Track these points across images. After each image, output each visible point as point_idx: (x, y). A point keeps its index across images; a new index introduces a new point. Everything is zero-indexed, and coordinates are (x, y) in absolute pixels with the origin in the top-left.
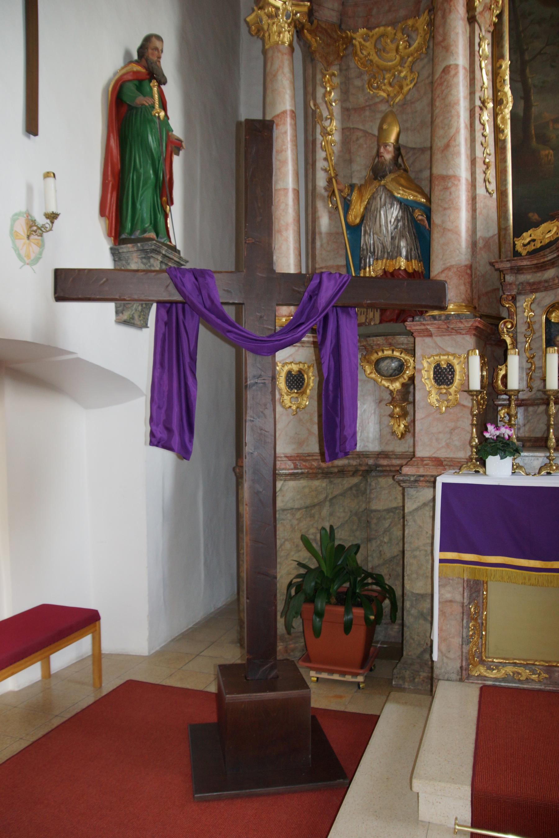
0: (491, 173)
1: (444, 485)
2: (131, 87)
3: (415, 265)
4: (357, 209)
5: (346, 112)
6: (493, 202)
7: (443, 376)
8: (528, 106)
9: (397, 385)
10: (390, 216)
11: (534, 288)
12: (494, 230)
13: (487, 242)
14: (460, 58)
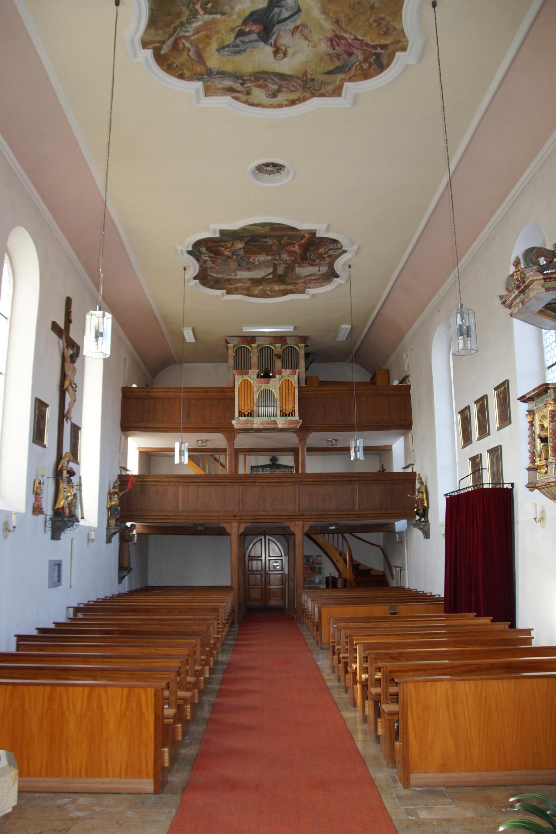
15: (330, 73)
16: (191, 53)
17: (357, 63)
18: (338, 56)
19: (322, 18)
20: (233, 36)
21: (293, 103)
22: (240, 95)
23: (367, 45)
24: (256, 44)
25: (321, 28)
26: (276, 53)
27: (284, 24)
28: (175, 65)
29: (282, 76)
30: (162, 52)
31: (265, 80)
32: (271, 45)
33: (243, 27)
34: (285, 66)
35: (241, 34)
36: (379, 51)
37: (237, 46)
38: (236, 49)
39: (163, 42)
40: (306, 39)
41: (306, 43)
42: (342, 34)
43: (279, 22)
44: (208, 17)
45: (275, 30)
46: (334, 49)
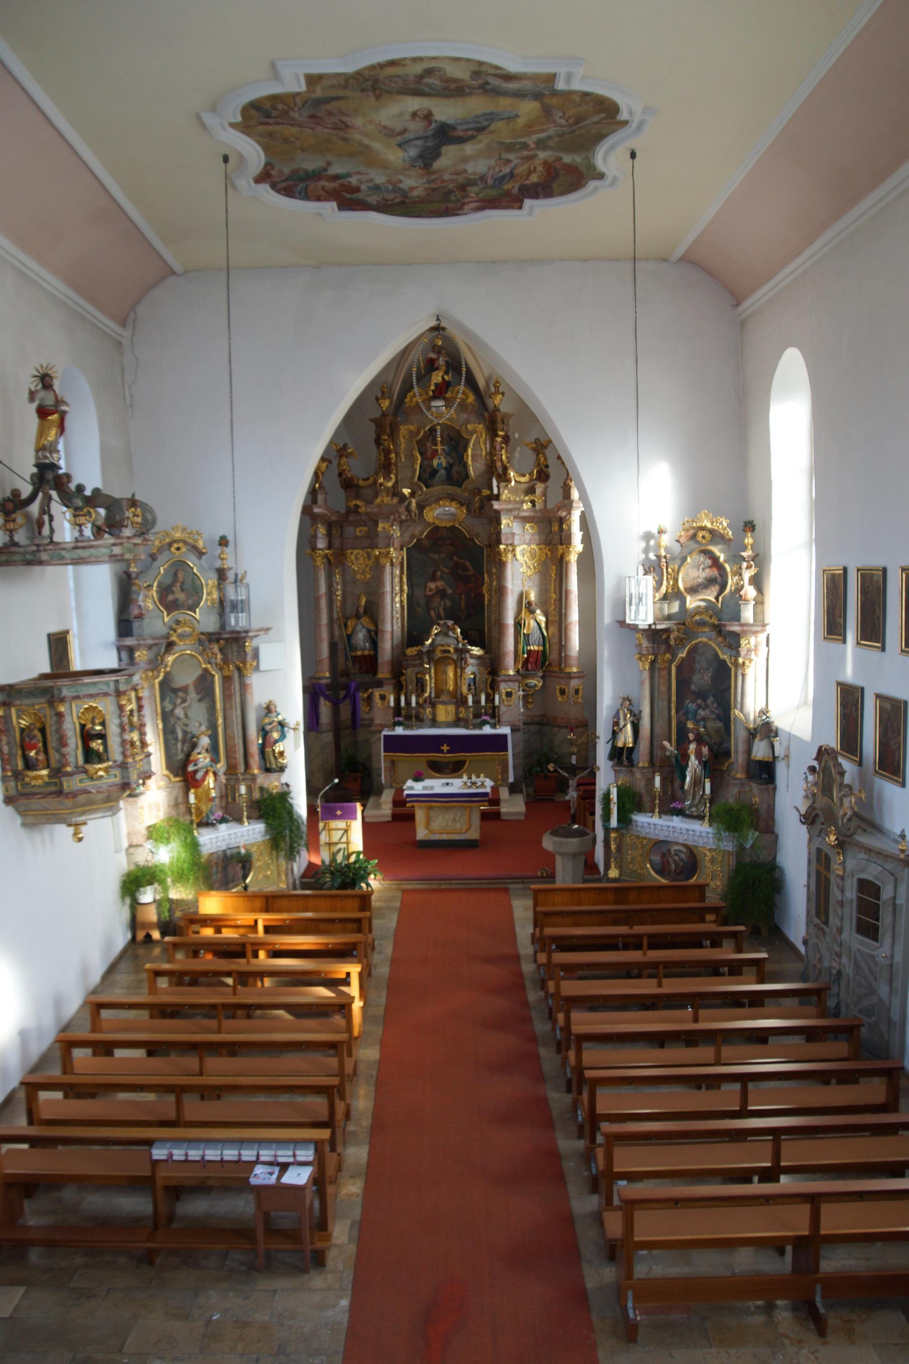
0: (399, 621)
1: (385, 736)
3: (372, 653)
4: (350, 630)
5: (344, 584)
6: (400, 630)
7: (383, 698)
9: (366, 695)
11: (413, 666)
12: (400, 640)
13: (397, 646)
15: (338, 98)
16: (561, 114)
17: (297, 108)
18: (330, 113)
19: (366, 141)
20: (492, 128)
21: (392, 63)
22: (493, 71)
23: (292, 125)
24: (459, 121)
25: (366, 134)
26: (428, 117)
27: (418, 136)
28: (592, 104)
29: (416, 93)
30: (603, 115)
31: (445, 88)
32: (436, 122)
33: (475, 133)
34: (413, 104)
35: (481, 130)
36: (271, 121)
37: (486, 120)
38: (491, 117)
39: (597, 123)
40: (385, 127)
41: (383, 123)
42: (335, 132)
43: (426, 138)
44: (523, 140)
45: (430, 133)
46: (341, 121)
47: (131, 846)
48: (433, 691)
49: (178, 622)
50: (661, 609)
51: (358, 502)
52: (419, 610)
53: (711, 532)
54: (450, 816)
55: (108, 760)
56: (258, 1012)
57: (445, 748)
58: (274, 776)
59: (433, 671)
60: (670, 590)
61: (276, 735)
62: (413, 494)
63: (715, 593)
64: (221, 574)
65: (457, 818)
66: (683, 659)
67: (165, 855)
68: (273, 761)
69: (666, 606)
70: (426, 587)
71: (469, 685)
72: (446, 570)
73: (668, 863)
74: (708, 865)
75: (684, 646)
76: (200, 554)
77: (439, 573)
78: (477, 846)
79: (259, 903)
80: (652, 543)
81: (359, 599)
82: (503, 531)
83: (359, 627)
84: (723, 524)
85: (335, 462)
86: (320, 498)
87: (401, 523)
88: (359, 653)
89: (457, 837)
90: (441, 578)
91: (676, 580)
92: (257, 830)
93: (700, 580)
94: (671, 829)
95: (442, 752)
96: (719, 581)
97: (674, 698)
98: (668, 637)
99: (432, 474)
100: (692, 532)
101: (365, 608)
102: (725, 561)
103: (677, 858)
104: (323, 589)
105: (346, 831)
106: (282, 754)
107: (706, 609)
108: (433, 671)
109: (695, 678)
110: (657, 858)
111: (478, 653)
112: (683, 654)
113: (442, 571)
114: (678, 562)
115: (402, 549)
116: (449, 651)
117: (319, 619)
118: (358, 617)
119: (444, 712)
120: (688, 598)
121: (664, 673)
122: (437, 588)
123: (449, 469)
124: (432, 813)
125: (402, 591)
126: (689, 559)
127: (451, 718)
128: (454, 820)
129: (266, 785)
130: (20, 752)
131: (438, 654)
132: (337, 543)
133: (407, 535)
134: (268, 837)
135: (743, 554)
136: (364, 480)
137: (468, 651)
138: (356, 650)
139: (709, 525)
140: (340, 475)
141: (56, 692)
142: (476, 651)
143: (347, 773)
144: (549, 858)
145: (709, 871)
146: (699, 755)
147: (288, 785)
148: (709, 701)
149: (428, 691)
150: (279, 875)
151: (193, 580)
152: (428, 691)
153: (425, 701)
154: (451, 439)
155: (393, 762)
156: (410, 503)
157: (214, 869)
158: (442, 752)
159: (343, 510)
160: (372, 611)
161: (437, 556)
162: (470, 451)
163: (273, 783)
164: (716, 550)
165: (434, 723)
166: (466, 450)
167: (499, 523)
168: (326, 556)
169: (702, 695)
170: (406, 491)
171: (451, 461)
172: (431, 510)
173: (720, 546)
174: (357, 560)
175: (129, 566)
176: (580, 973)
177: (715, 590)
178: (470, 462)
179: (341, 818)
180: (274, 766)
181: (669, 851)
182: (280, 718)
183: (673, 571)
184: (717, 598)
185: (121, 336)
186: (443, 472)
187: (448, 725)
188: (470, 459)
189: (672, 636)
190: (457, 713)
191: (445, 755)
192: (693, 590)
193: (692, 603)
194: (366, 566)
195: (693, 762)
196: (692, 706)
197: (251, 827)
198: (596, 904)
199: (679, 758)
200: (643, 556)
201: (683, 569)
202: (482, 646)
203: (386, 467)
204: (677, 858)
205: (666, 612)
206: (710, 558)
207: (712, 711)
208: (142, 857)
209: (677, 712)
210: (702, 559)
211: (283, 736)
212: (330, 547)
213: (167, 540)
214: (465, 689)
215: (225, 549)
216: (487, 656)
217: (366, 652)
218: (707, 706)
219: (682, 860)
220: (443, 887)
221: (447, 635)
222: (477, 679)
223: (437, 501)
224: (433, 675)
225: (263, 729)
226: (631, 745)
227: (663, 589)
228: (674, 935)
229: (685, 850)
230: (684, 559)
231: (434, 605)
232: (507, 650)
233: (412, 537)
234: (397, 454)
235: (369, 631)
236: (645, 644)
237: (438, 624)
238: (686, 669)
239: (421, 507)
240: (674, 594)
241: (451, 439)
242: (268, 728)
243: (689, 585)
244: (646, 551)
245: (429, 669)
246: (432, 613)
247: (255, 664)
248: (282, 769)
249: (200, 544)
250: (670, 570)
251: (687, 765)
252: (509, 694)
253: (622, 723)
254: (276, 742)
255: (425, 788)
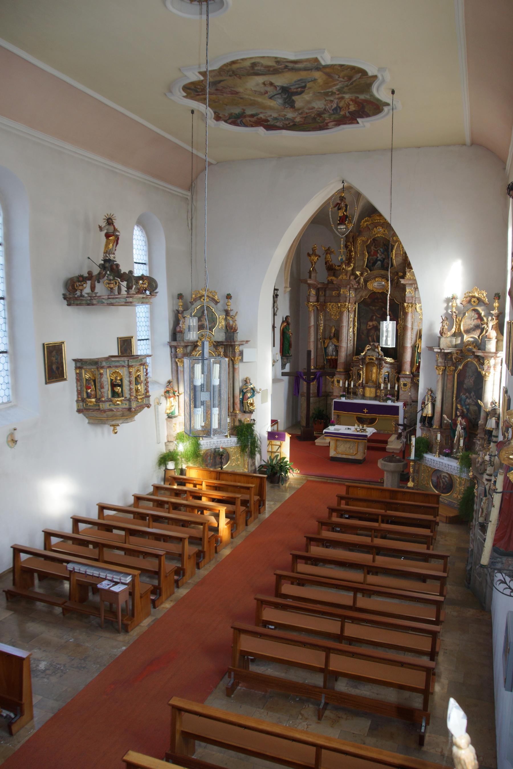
2: (285, 330)
5: (325, 321)
7: (338, 382)
8: (360, 327)
10: (331, 348)
11: (356, 366)
13: (350, 355)
14: (345, 324)
47: (168, 441)
48: (364, 379)
49: (202, 336)
50: (451, 342)
51: (333, 278)
52: (363, 336)
53: (478, 299)
54: (348, 445)
55: (123, 396)
56: (193, 525)
57: (365, 411)
58: (247, 415)
59: (364, 369)
60: (457, 331)
61: (249, 395)
62: (362, 274)
63: (478, 334)
64: (227, 313)
65: (351, 447)
66: (461, 370)
67: (183, 448)
68: (247, 407)
69: (454, 339)
70: (367, 324)
71: (385, 378)
72: (379, 316)
73: (440, 482)
74: (458, 485)
75: (461, 363)
76: (217, 303)
77: (374, 317)
78: (360, 463)
79: (214, 475)
80: (450, 304)
81: (331, 328)
82: (407, 296)
83: (330, 344)
84: (483, 295)
85: (323, 257)
86: (313, 275)
87: (356, 290)
88: (329, 357)
89: (350, 457)
90: (376, 320)
91: (460, 326)
92: (233, 441)
93: (472, 326)
94: (441, 464)
95: (364, 412)
96: (480, 327)
97: (455, 392)
98: (452, 358)
99: (351, 264)
100: (469, 298)
101: (334, 334)
102: (484, 316)
103: (444, 480)
104: (312, 323)
105: (280, 446)
106: (252, 404)
107: (473, 342)
108: (364, 369)
109: (466, 381)
110: (435, 479)
111: (391, 361)
112: (460, 367)
113: (376, 316)
114: (462, 315)
115: (355, 303)
116: (373, 359)
117: (310, 338)
118: (330, 339)
119: (370, 392)
120: (465, 336)
121: (450, 377)
122: (373, 325)
123: (382, 261)
124: (338, 443)
125: (354, 325)
126: (467, 314)
127: (373, 395)
128: (349, 448)
129: (243, 420)
130: (85, 390)
131: (367, 361)
132: (322, 299)
133: (359, 296)
134: (238, 445)
135: (491, 312)
136: (338, 266)
137: (383, 360)
138: (328, 356)
139: (477, 295)
140: (326, 263)
141: (99, 364)
142: (389, 360)
143: (316, 419)
144: (382, 472)
145: (458, 489)
146: (461, 424)
147: (254, 420)
148: (472, 395)
149: (362, 380)
150: (244, 464)
151: (212, 315)
152: (362, 380)
153: (359, 385)
154: (384, 245)
155: (338, 416)
156: (360, 279)
157: (209, 457)
158: (364, 412)
159: (326, 282)
160: (337, 336)
161: (374, 308)
162: (394, 251)
163: (246, 419)
164: (480, 309)
165: (363, 397)
166: (392, 251)
167: (405, 291)
168: (314, 306)
169: (468, 390)
170: (358, 273)
171: (384, 257)
172: (371, 283)
173: (482, 307)
174: (331, 307)
175: (179, 308)
176: (359, 532)
177: (478, 332)
178: (394, 258)
179: (278, 439)
180: (247, 410)
181: (440, 476)
182: (252, 386)
183: (459, 320)
184: (479, 337)
185: (187, 195)
186: (379, 262)
187: (371, 399)
188: (394, 256)
189: (453, 357)
190: (376, 393)
191: (366, 414)
192: (468, 332)
193: (467, 338)
194: (337, 312)
195: (459, 428)
196: (464, 397)
197: (231, 439)
198: (421, 502)
199: (452, 425)
200: (445, 311)
201: (463, 320)
202: (393, 358)
203: (349, 260)
204: (444, 480)
205: (454, 343)
206: (477, 314)
207: (473, 400)
208: (172, 447)
209: (456, 399)
210: (473, 314)
211: (253, 395)
212: (318, 301)
213: (199, 295)
214: (381, 380)
215: (229, 300)
216: (396, 363)
217: (333, 357)
218: (471, 397)
219: (446, 481)
220: (328, 481)
221: (374, 351)
222: (390, 375)
223: (375, 278)
224: (364, 372)
225: (243, 391)
226: (430, 416)
227: (453, 330)
228: (396, 517)
229: (448, 476)
230: (464, 314)
231: (371, 334)
232: (406, 361)
233: (361, 297)
234: (355, 253)
235: (336, 346)
236: (440, 360)
237: (370, 345)
238: (462, 375)
239: (366, 281)
240: (458, 334)
241: (384, 245)
242: (245, 391)
243: (466, 328)
244: (447, 308)
245: (363, 368)
246: (370, 338)
247: (240, 358)
248: (251, 412)
249: (216, 298)
250: (457, 320)
251: (456, 430)
252: (405, 385)
253: (426, 403)
254: (249, 398)
255: (335, 429)
